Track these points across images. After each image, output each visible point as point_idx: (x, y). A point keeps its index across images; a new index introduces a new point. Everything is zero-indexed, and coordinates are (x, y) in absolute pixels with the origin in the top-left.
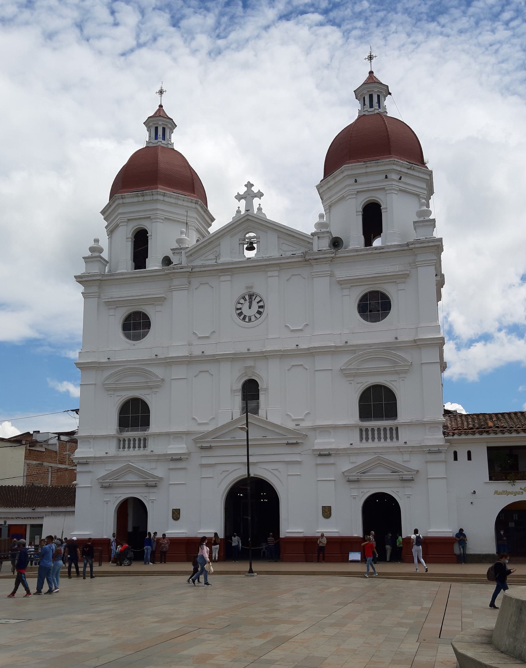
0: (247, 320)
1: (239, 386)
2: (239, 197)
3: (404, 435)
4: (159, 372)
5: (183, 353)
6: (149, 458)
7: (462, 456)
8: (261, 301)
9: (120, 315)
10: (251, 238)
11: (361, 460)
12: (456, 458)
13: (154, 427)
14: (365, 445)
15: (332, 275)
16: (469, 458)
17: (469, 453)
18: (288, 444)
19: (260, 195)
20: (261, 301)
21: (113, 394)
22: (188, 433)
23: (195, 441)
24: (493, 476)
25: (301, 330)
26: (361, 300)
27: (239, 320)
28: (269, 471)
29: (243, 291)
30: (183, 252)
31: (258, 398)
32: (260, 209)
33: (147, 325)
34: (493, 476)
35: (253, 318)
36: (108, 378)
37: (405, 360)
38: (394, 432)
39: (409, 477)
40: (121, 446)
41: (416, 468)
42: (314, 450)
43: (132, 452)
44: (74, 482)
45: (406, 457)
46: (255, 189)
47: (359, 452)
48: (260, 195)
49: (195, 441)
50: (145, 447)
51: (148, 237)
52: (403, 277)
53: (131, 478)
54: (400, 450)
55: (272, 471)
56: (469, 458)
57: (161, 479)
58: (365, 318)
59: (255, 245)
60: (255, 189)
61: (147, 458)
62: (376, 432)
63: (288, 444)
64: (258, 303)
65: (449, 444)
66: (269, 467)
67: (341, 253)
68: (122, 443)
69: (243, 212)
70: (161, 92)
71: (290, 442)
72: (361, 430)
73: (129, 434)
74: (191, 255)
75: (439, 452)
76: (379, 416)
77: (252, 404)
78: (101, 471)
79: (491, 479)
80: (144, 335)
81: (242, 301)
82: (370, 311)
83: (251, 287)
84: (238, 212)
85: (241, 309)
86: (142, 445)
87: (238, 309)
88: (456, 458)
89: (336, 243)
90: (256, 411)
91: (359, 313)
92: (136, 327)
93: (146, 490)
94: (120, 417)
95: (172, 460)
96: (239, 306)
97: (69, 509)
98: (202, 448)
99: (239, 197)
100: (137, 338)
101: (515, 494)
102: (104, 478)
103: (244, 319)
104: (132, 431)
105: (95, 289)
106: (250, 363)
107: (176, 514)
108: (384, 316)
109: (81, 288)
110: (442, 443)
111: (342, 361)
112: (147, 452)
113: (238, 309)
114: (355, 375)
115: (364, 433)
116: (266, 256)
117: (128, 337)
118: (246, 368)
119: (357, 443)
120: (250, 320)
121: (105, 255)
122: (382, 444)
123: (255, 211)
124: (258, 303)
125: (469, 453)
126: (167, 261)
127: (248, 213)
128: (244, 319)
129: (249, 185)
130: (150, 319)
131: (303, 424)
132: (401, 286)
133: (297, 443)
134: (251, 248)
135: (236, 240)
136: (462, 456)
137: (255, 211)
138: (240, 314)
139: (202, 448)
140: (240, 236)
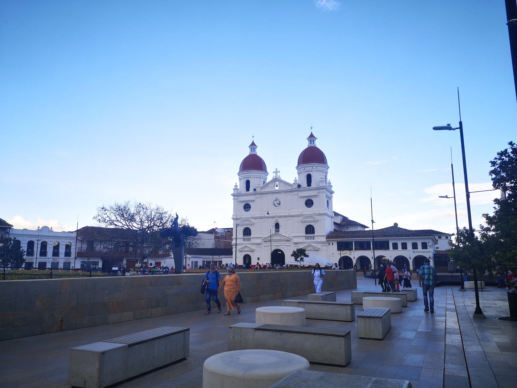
0: (276, 206)
1: (274, 225)
2: (274, 173)
4: (253, 221)
7: (331, 244)
9: (243, 204)
10: (277, 184)
13: (252, 236)
14: (307, 241)
15: (298, 195)
18: (287, 241)
19: (279, 172)
22: (261, 237)
25: (290, 210)
27: (274, 206)
30: (259, 187)
31: (279, 228)
32: (279, 176)
33: (250, 207)
35: (278, 206)
36: (240, 222)
37: (316, 218)
39: (317, 250)
41: (319, 247)
44: (232, 250)
46: (278, 170)
47: (305, 243)
48: (279, 172)
50: (250, 241)
52: (316, 196)
54: (315, 242)
57: (254, 249)
59: (278, 186)
60: (278, 170)
62: (310, 237)
63: (287, 241)
67: (300, 189)
68: (244, 240)
69: (275, 177)
71: (287, 240)
72: (306, 237)
75: (325, 243)
76: (310, 233)
77: (278, 229)
79: (338, 250)
80: (249, 210)
81: (275, 201)
83: (277, 198)
84: (274, 176)
89: (299, 186)
90: (278, 231)
95: (257, 244)
96: (274, 203)
97: (231, 256)
98: (265, 241)
99: (274, 173)
100: (247, 211)
101: (343, 254)
103: (275, 206)
104: (247, 236)
105: (236, 198)
106: (277, 219)
109: (232, 197)
114: (304, 222)
115: (307, 238)
116: (280, 189)
117: (245, 210)
118: (276, 220)
120: (277, 206)
121: (238, 187)
123: (278, 176)
126: (255, 190)
127: (276, 177)
128: (275, 206)
129: (276, 169)
131: (291, 235)
132: (316, 198)
133: (289, 241)
134: (277, 186)
135: (273, 184)
136: (331, 244)
137: (278, 176)
138: (274, 205)
139: (265, 241)
140: (274, 183)
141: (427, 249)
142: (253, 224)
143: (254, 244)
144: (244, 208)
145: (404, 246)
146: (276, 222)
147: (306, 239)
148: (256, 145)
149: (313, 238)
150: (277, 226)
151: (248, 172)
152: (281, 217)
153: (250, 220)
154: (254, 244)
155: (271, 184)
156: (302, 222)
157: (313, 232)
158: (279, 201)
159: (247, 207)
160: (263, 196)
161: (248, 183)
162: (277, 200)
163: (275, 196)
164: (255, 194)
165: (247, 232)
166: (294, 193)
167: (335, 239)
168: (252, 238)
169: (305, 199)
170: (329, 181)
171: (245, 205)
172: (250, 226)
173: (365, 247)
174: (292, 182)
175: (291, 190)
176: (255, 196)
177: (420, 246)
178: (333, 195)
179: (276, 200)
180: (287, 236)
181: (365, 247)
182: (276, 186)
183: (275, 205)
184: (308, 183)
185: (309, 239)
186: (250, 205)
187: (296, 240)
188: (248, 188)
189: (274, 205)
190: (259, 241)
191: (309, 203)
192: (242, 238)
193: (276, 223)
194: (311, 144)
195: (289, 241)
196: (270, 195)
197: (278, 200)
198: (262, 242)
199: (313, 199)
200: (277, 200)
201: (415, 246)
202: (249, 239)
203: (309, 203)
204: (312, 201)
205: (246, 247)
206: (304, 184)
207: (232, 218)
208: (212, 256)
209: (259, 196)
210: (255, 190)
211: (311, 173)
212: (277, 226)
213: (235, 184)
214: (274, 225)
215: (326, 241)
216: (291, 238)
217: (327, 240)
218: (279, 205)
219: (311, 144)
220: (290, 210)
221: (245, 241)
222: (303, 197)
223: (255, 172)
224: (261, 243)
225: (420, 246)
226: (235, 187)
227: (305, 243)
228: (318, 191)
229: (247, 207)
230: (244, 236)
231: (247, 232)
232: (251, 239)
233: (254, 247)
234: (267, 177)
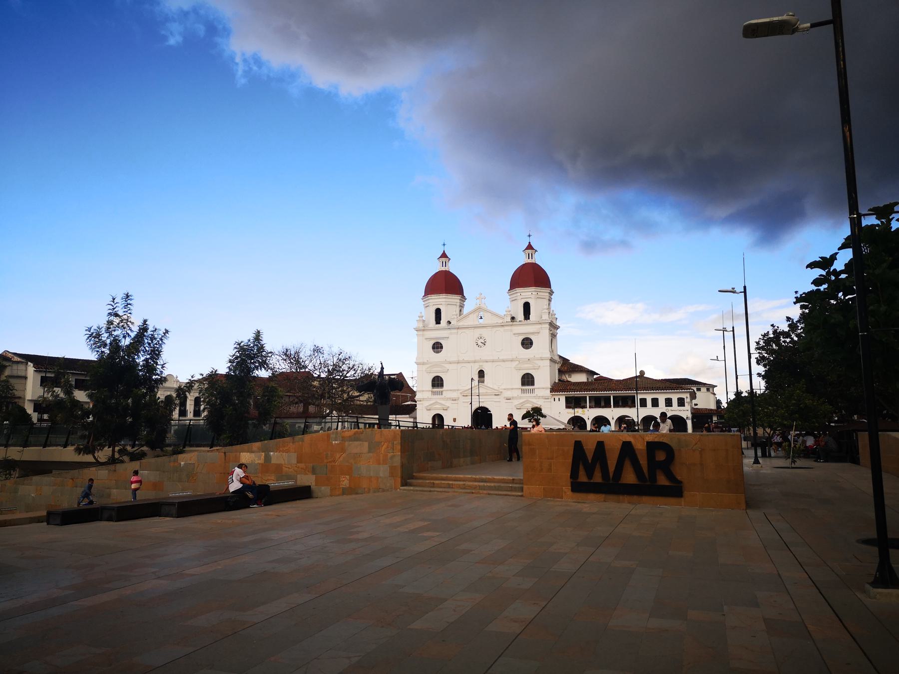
3: (537, 392)
4: (447, 366)
5: (456, 359)
9: (433, 342)
11: (521, 401)
14: (523, 395)
16: (559, 400)
18: (495, 395)
23: (461, 393)
24: (567, 407)
26: (522, 341)
29: (478, 336)
33: (442, 347)
34: (567, 407)
36: (428, 368)
42: (505, 397)
49: (461, 393)
53: (437, 406)
56: (559, 400)
57: (448, 407)
58: (524, 347)
61: (443, 399)
63: (495, 395)
66: (488, 403)
67: (514, 323)
68: (434, 393)
73: (436, 390)
76: (528, 385)
77: (482, 379)
78: (426, 403)
89: (513, 318)
90: (483, 382)
93: (443, 411)
98: (463, 396)
100: (438, 352)
102: (427, 406)
105: (421, 333)
106: (481, 364)
107: (455, 420)
108: (531, 347)
110: (550, 395)
111: (515, 364)
112: (443, 396)
114: (520, 370)
118: (480, 366)
122: (529, 395)
126: (449, 322)
131: (501, 388)
133: (498, 395)
139: (463, 396)
140: (477, 314)
141: (684, 406)
143: (448, 399)
144: (433, 348)
145: (655, 403)
148: (448, 257)
149: (533, 391)
150: (481, 374)
151: (438, 297)
152: (487, 362)
153: (443, 365)
154: (448, 399)
155: (472, 314)
156: (517, 370)
157: (532, 384)
159: (437, 347)
160: (460, 331)
161: (438, 312)
163: (478, 332)
165: (437, 382)
167: (563, 393)
168: (445, 390)
170: (553, 311)
171: (434, 344)
173: (603, 404)
174: (502, 313)
175: (502, 324)
176: (449, 331)
177: (675, 402)
178: (558, 331)
180: (496, 387)
181: (603, 404)
182: (479, 317)
183: (479, 344)
184: (525, 315)
185: (528, 393)
186: (441, 344)
187: (508, 394)
188: (438, 320)
189: (477, 344)
190: (455, 395)
191: (527, 343)
194: (529, 259)
195: (498, 395)
196: (470, 331)
198: (460, 396)
199: (532, 337)
201: (669, 402)
203: (527, 343)
204: (531, 340)
205: (436, 403)
206: (520, 316)
207: (415, 362)
208: (395, 416)
209: (455, 331)
210: (449, 322)
212: (481, 374)
213: (419, 314)
216: (501, 391)
218: (485, 344)
219: (529, 259)
222: (519, 334)
223: (448, 297)
224: (458, 398)
225: (675, 402)
226: (419, 318)
227: (520, 399)
228: (540, 326)
229: (437, 347)
230: (433, 388)
231: (437, 382)
232: (444, 393)
233: (448, 404)
234: (465, 303)
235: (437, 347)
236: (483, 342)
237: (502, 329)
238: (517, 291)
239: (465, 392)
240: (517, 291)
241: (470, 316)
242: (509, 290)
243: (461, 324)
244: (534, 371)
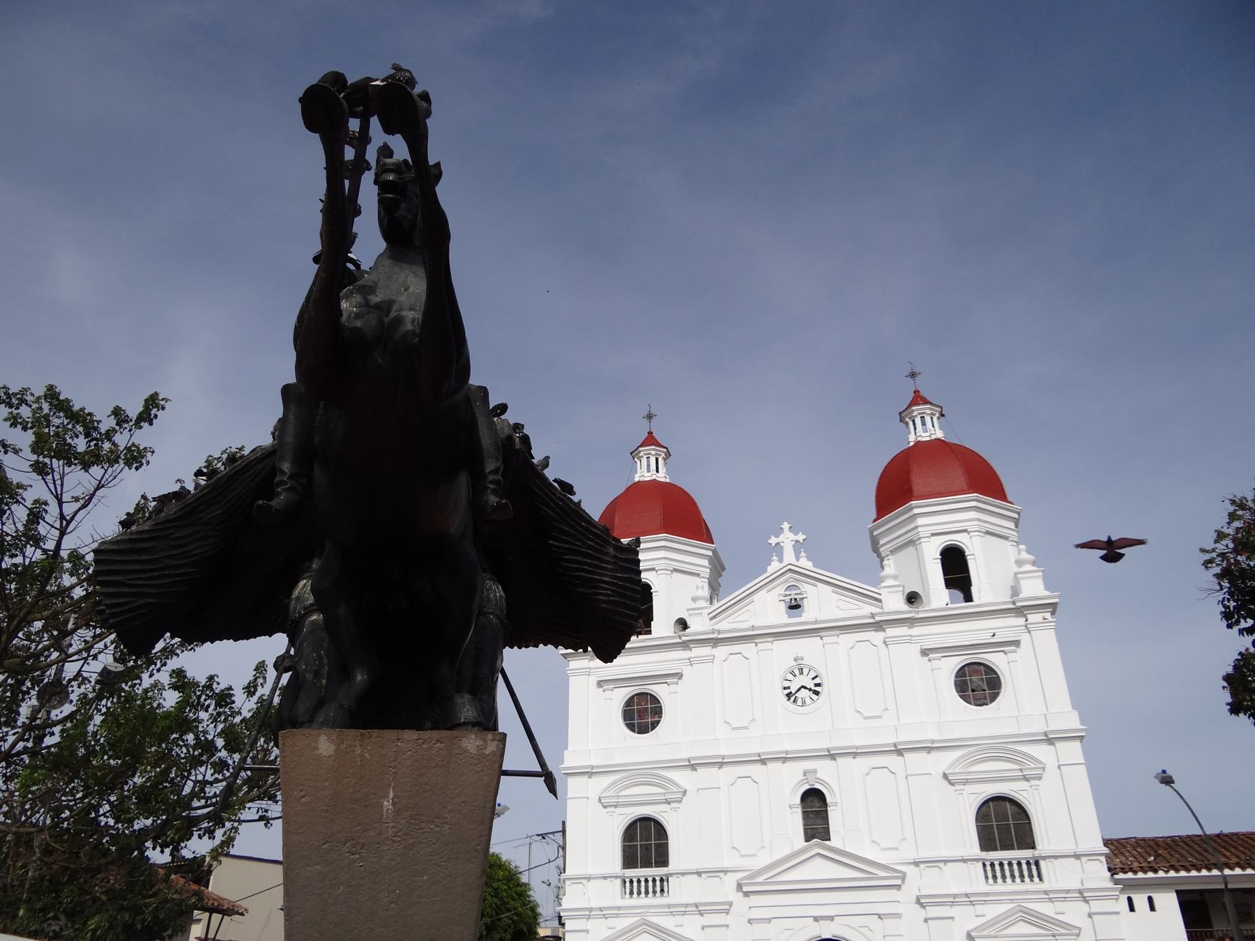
0: (799, 702)
4: (683, 778)
6: (672, 910)
8: (816, 677)
11: (992, 911)
12: (1132, 909)
16: (1152, 908)
17: (1150, 900)
20: (816, 677)
21: (614, 812)
25: (879, 717)
26: (957, 675)
28: (856, 930)
33: (658, 711)
35: (808, 701)
38: (1034, 867)
40: (628, 890)
43: (643, 900)
45: (1060, 906)
51: (651, 594)
55: (859, 929)
56: (1152, 908)
61: (673, 911)
64: (813, 679)
65: (1121, 886)
68: (631, 887)
70: (650, 417)
72: (984, 865)
74: (715, 617)
81: (790, 677)
82: (973, 691)
85: (789, 688)
86: (658, 889)
87: (785, 688)
88: (1132, 909)
90: (826, 835)
91: (958, 692)
92: (642, 713)
94: (624, 845)
96: (787, 684)
108: (994, 697)
113: (785, 688)
119: (982, 886)
120: (804, 703)
122: (1018, 886)
124: (813, 679)
125: (1150, 900)
128: (795, 701)
130: (660, 703)
142: (676, 798)
146: (800, 783)
147: (987, 878)
158: (813, 674)
160: (722, 651)
162: (801, 673)
163: (785, 651)
164: (685, 645)
166: (891, 631)
169: (954, 664)
171: (630, 702)
172: (665, 807)
179: (797, 672)
187: (921, 882)
192: (616, 877)
193: (807, 787)
197: (806, 671)
200: (801, 673)
202: (639, 881)
204: (989, 670)
209: (706, 651)
210: (682, 624)
211: (962, 540)
214: (798, 800)
215: (1111, 885)
217: (1117, 882)
218: (817, 693)
220: (879, 717)
221: (631, 893)
235: (639, 711)
236: (811, 685)
237: (876, 637)
238: (916, 511)
239: (760, 879)
240: (916, 511)
241: (756, 597)
242: (875, 521)
243: (726, 625)
244: (1024, 785)
